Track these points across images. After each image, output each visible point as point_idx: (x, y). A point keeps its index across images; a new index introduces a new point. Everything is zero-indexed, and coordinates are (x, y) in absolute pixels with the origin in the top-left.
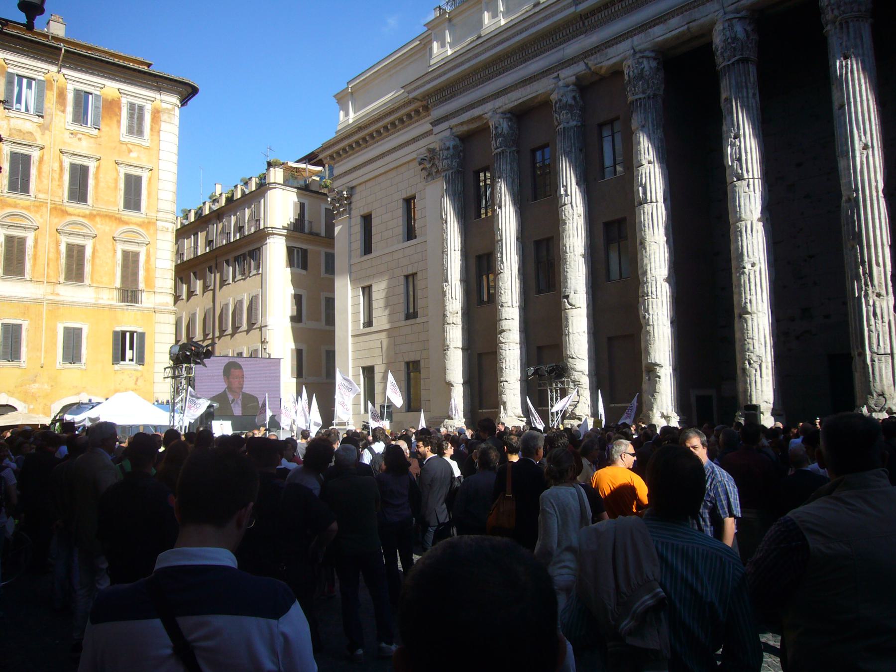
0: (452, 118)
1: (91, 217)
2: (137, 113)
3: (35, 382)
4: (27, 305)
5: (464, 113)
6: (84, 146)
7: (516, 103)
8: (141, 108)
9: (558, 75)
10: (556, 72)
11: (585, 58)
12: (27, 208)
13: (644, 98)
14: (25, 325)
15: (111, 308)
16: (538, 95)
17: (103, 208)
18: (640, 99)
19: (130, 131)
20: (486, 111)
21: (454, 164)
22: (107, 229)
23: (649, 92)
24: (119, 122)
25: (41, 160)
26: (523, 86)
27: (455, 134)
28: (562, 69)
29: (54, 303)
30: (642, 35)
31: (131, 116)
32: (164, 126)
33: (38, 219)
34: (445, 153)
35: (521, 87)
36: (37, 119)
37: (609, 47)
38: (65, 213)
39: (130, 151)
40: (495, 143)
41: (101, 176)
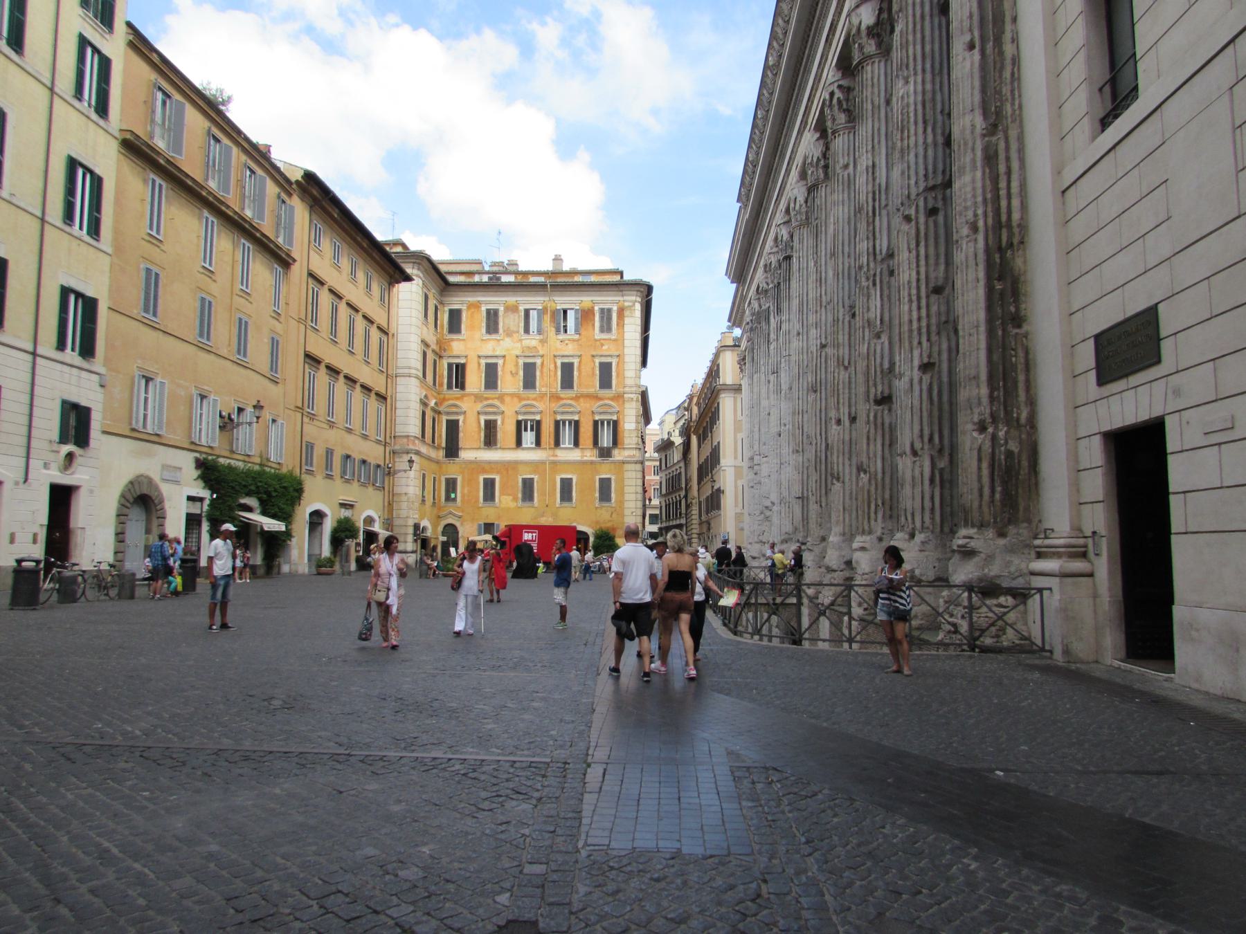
1: (577, 398)
2: (606, 314)
3: (543, 516)
4: (537, 465)
6: (570, 349)
8: (609, 310)
12: (534, 399)
14: (536, 478)
15: (592, 463)
17: (585, 391)
19: (602, 330)
22: (588, 405)
23: (776, 282)
24: (594, 325)
25: (542, 364)
29: (554, 463)
31: (602, 318)
32: (627, 320)
33: (540, 406)
36: (538, 337)
38: (559, 398)
39: (602, 345)
41: (583, 367)
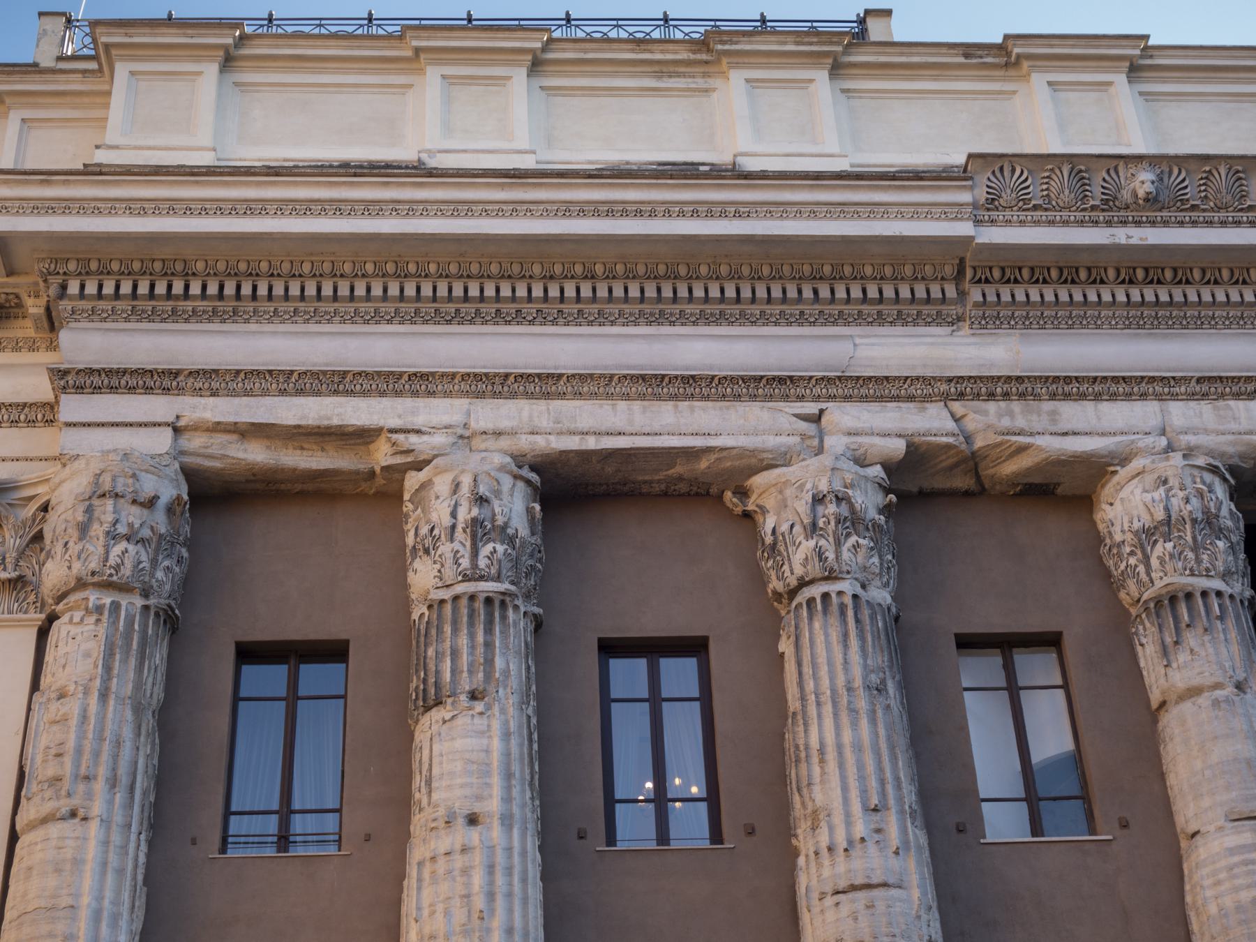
0: (198, 392)
5: (283, 392)
7: (591, 443)
9: (822, 411)
10: (817, 399)
11: (961, 396)
13: (1231, 596)
16: (709, 450)
18: (1219, 594)
20: (419, 421)
21: (160, 574)
26: (642, 397)
27: (187, 460)
28: (847, 398)
30: (1205, 408)
34: (134, 515)
35: (627, 397)
37: (1067, 397)
40: (466, 552)
